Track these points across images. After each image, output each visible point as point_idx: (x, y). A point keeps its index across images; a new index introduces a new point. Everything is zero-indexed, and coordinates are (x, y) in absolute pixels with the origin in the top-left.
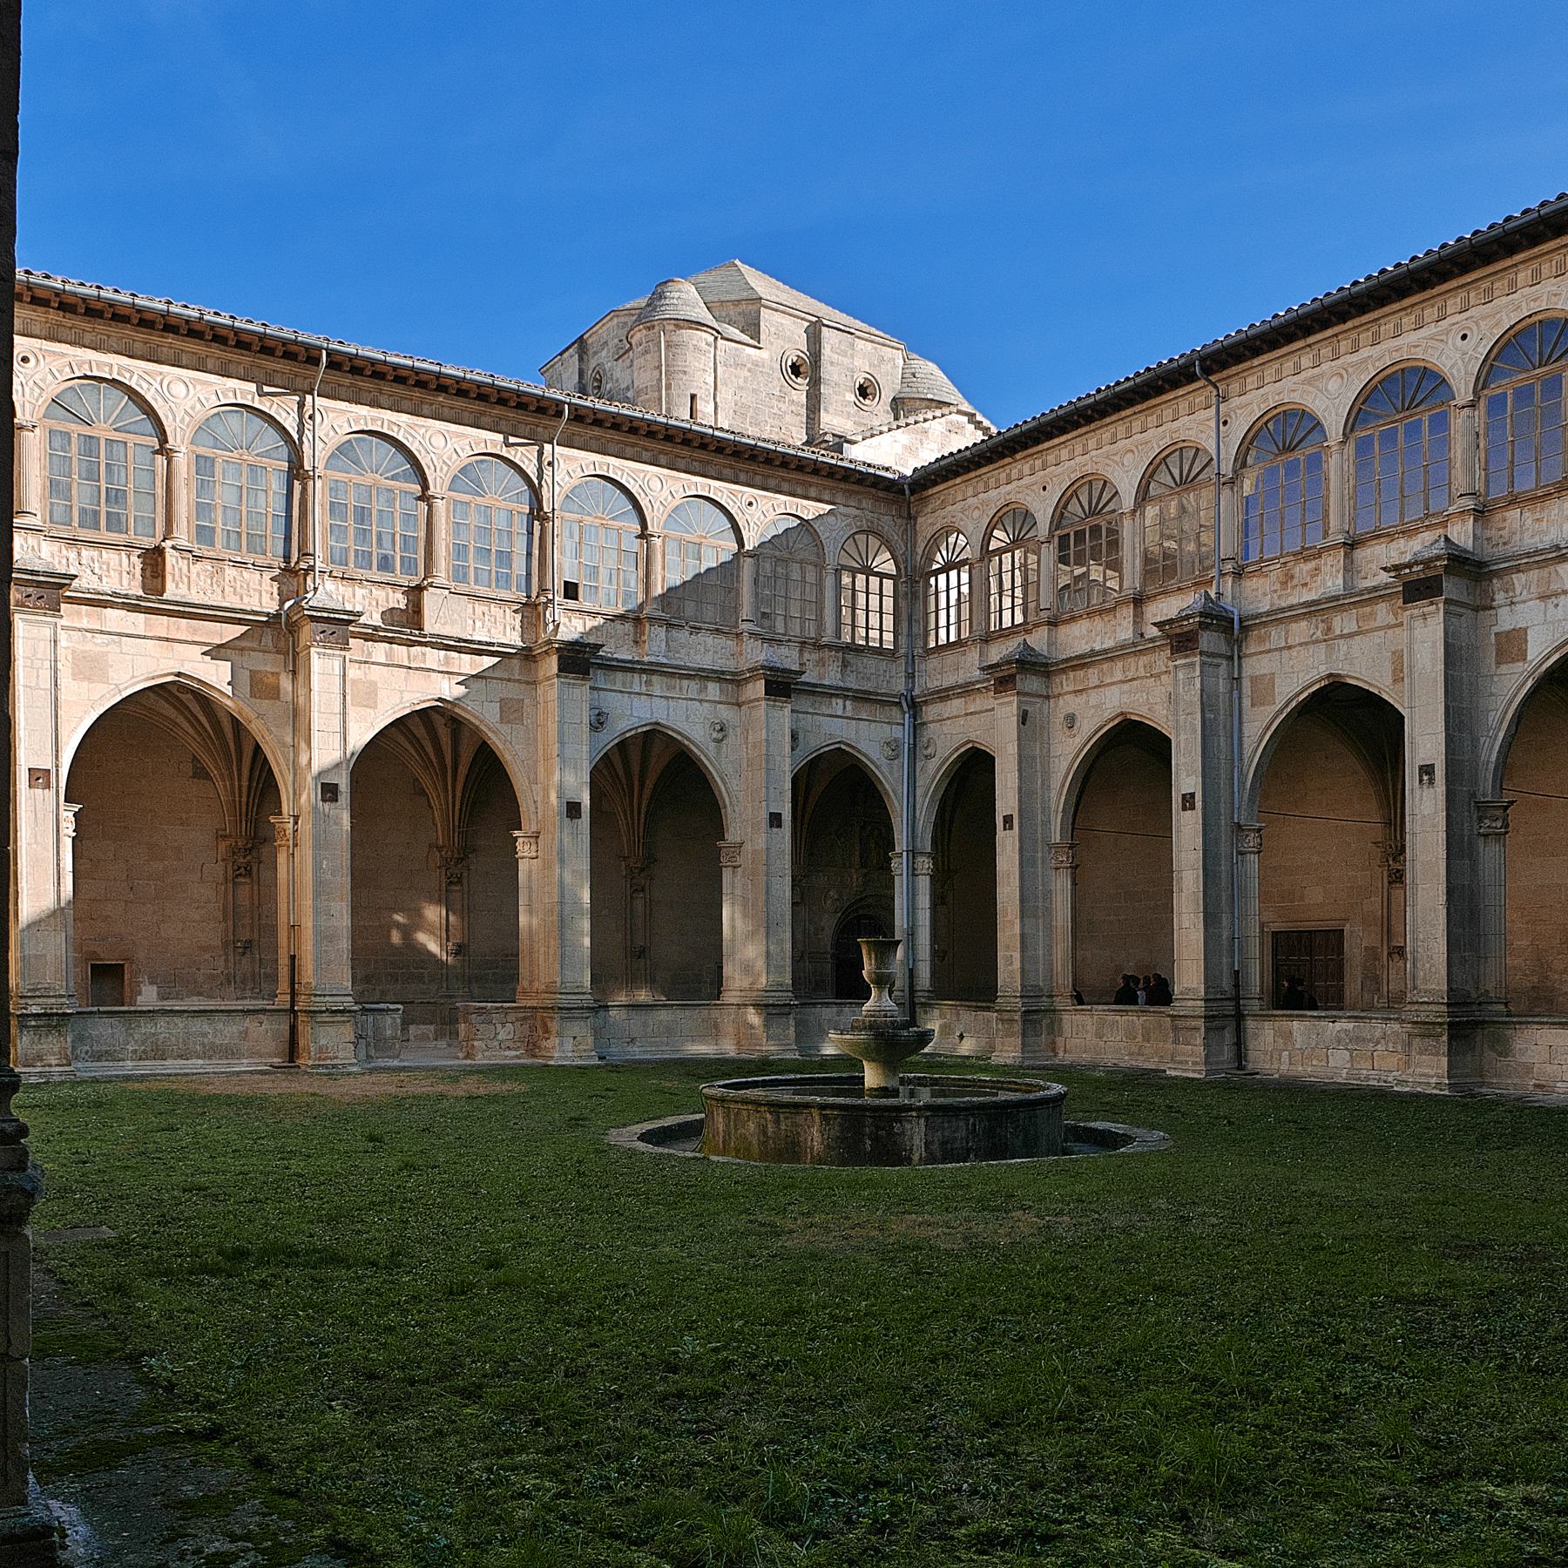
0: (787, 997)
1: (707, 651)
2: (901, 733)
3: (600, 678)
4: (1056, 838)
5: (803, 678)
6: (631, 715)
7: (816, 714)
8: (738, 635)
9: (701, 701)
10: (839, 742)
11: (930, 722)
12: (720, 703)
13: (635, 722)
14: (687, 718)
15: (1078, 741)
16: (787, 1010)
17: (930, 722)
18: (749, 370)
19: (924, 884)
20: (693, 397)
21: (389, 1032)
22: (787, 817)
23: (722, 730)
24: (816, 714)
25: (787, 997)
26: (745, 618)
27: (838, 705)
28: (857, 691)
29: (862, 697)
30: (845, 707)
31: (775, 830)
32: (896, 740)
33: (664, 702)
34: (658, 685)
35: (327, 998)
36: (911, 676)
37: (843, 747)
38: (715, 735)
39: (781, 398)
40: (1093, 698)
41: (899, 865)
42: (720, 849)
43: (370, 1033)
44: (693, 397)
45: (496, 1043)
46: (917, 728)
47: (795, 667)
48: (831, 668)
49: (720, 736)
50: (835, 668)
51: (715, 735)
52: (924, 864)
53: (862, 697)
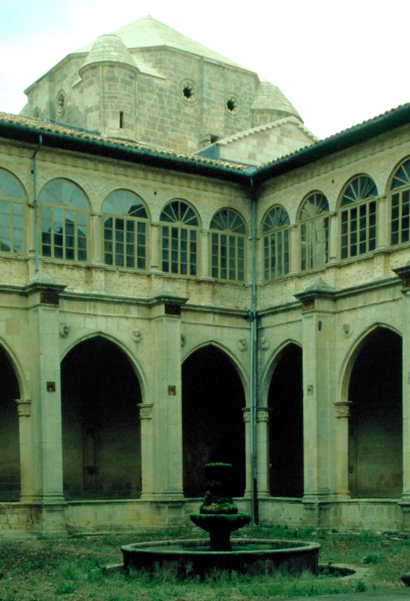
0: (181, 497)
1: (130, 286)
2: (249, 336)
3: (65, 305)
4: (339, 398)
5: (188, 302)
6: (85, 327)
7: (196, 324)
8: (149, 276)
9: (126, 318)
10: (211, 341)
11: (268, 327)
12: (138, 318)
14: (118, 328)
15: (351, 340)
16: (180, 505)
17: (268, 327)
18: (158, 94)
19: (263, 428)
20: (121, 114)
23: (139, 335)
24: (196, 324)
25: (181, 497)
26: (152, 265)
27: (210, 319)
28: (223, 309)
29: (225, 313)
30: (214, 319)
31: (172, 396)
32: (245, 340)
33: (104, 319)
34: (100, 309)
36: (255, 300)
37: (214, 344)
38: (135, 339)
39: (178, 112)
40: (360, 314)
41: (248, 416)
42: (140, 408)
44: (121, 114)
45: (7, 526)
46: (259, 331)
47: (184, 296)
49: (138, 339)
51: (135, 339)
52: (264, 415)
53: (225, 313)
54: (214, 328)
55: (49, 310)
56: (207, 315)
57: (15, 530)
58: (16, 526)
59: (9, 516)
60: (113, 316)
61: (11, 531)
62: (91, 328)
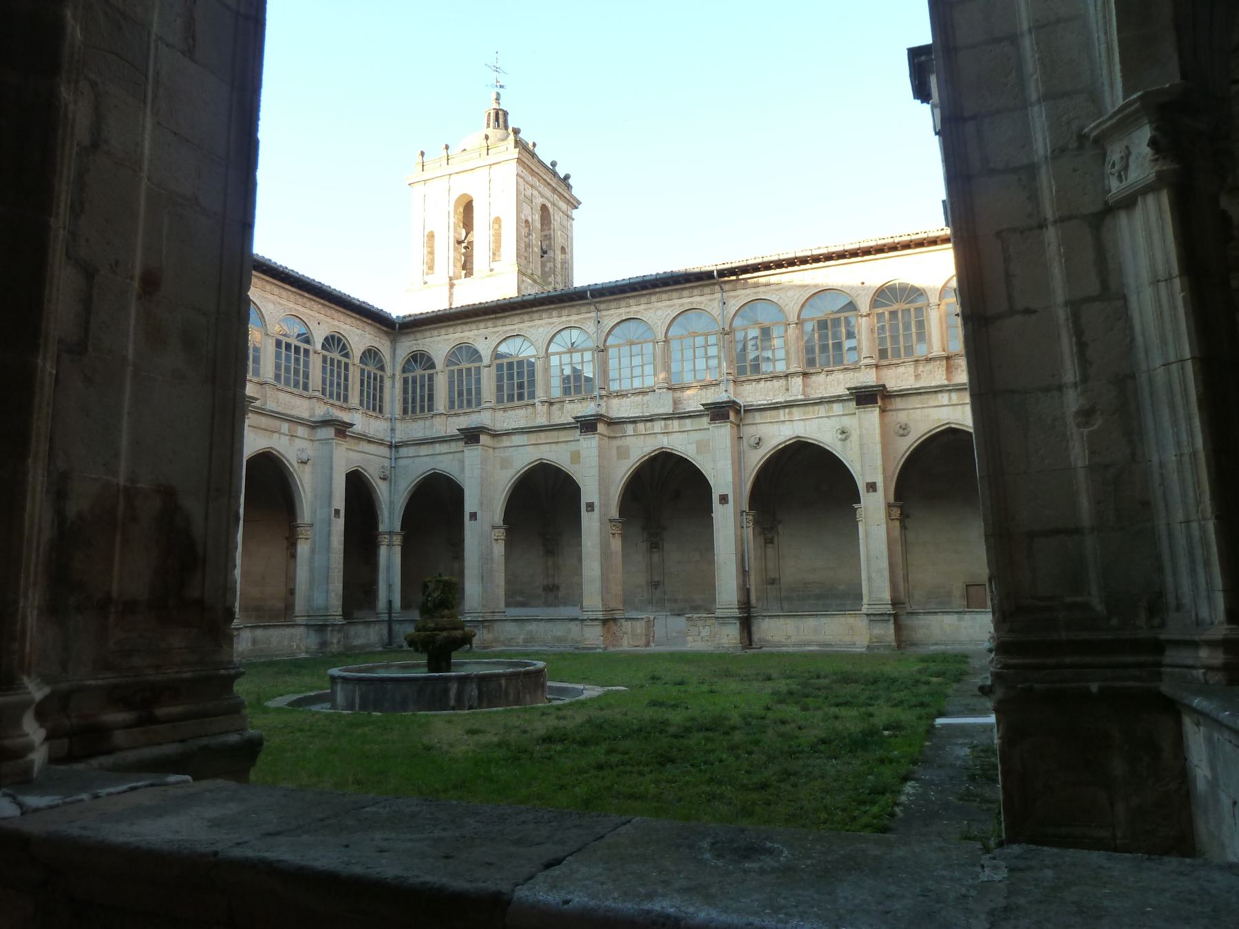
6: (780, 435)
7: (923, 408)
9: (828, 417)
12: (844, 415)
13: (782, 439)
21: (639, 631)
22: (880, 485)
24: (923, 408)
30: (950, 398)
33: (802, 423)
34: (797, 413)
35: (590, 613)
38: (840, 436)
43: (630, 632)
45: (699, 638)
48: (936, 373)
50: (940, 372)
54: (951, 407)
55: (721, 426)
56: (940, 396)
57: (707, 642)
58: (706, 638)
59: (701, 628)
60: (812, 418)
61: (703, 644)
62: (787, 434)
